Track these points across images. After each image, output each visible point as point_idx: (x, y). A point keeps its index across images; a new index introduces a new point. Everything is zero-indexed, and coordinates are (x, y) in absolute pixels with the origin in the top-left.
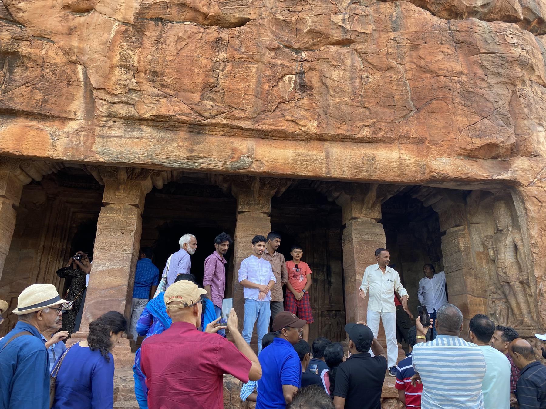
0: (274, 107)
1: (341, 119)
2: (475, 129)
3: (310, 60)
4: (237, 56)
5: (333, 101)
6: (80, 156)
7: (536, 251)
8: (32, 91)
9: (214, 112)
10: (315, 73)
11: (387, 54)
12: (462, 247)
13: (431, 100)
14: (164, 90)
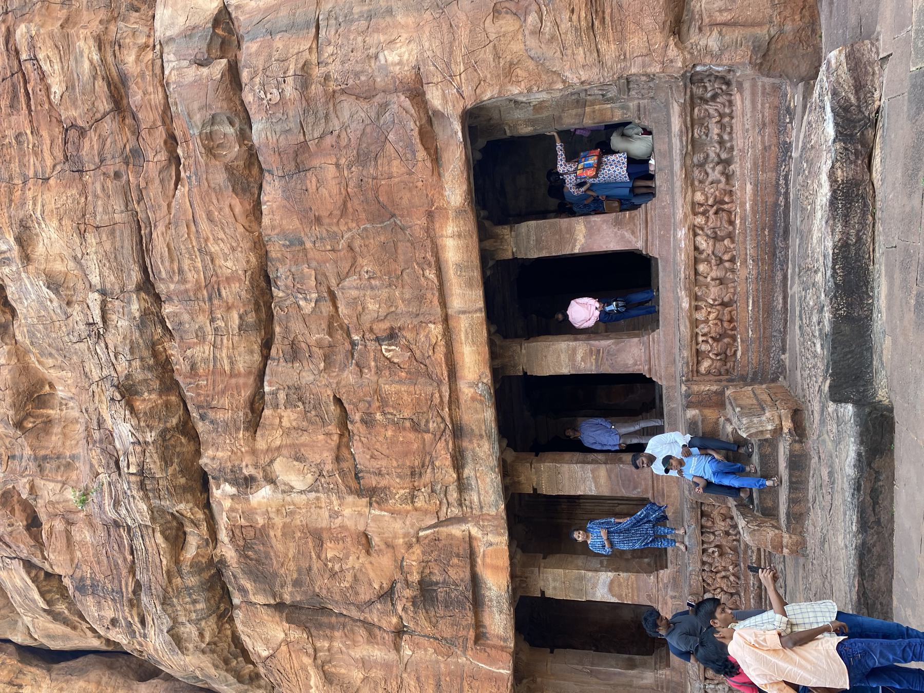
1: (421, 299)
2: (405, 154)
4: (377, 404)
5: (402, 307)
6: (503, 523)
9: (439, 420)
10: (374, 327)
11: (333, 250)
13: (379, 202)
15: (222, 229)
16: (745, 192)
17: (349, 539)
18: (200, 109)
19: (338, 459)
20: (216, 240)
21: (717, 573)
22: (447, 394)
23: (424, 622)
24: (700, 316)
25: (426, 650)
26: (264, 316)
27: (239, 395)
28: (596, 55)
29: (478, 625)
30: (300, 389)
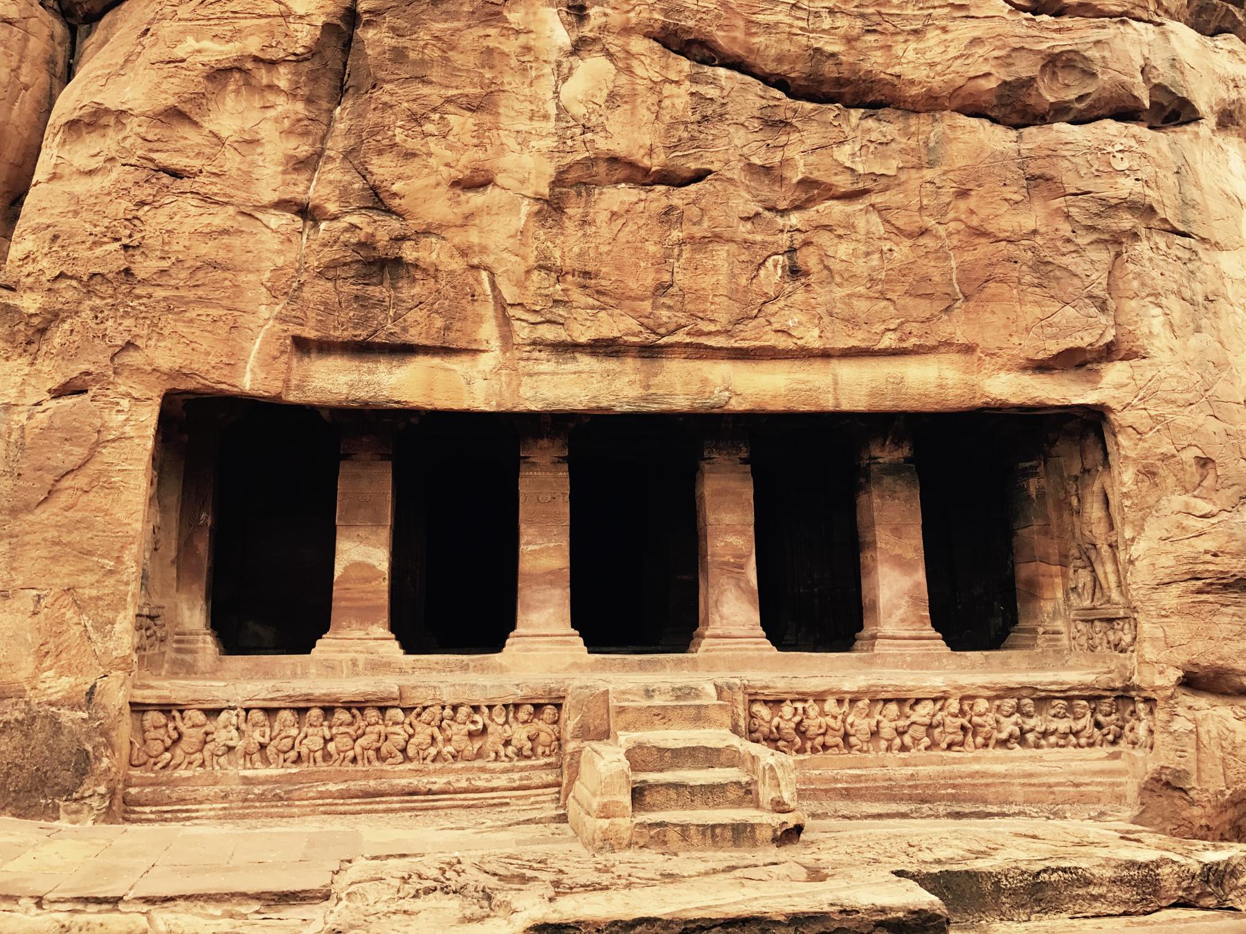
1: (851, 321)
2: (1050, 325)
3: (803, 229)
6: (508, 406)
7: (1127, 503)
9: (672, 327)
10: (811, 249)
11: (921, 208)
12: (1033, 491)
13: (987, 281)
14: (602, 299)
15: (962, 56)
16: (995, 762)
17: (480, 155)
18: (1104, 58)
19: (614, 160)
20: (946, 44)
21: (439, 727)
23: (329, 255)
24: (830, 705)
25: (280, 252)
26: (825, 89)
27: (719, 27)
28: (1167, 580)
29: (325, 347)
30: (721, 121)
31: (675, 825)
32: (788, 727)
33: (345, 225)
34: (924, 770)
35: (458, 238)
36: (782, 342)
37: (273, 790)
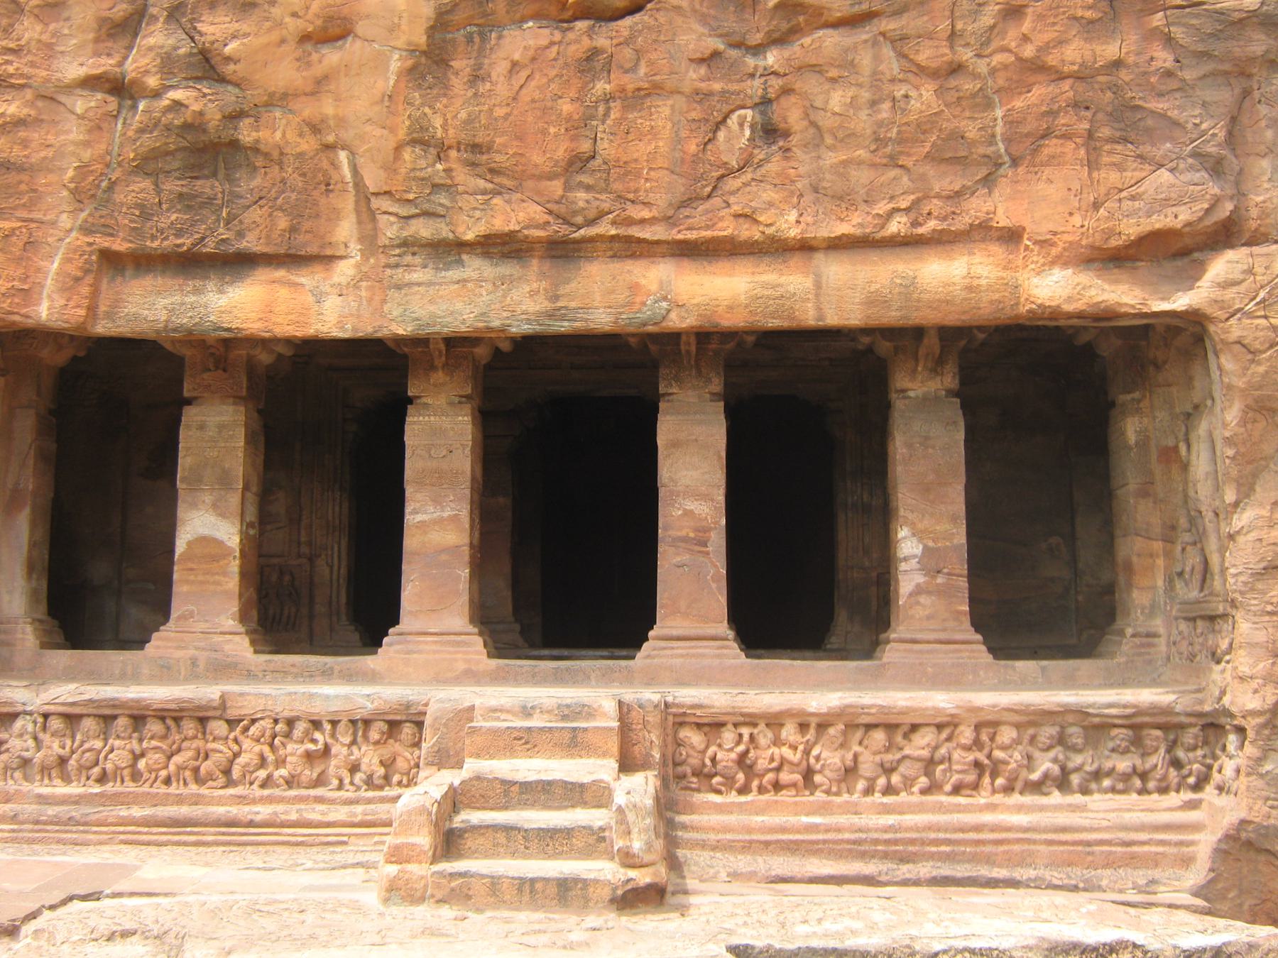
0: (709, 189)
2: (1133, 198)
3: (782, 71)
8: (270, 215)
9: (591, 215)
12: (1132, 437)
13: (1043, 137)
14: (496, 180)
21: (271, 745)
22: (642, 235)
23: (149, 141)
24: (789, 732)
25: (87, 144)
29: (144, 262)
31: (483, 876)
32: (727, 758)
33: (166, 102)
34: (909, 819)
35: (308, 110)
36: (748, 232)
37: (69, 811)
